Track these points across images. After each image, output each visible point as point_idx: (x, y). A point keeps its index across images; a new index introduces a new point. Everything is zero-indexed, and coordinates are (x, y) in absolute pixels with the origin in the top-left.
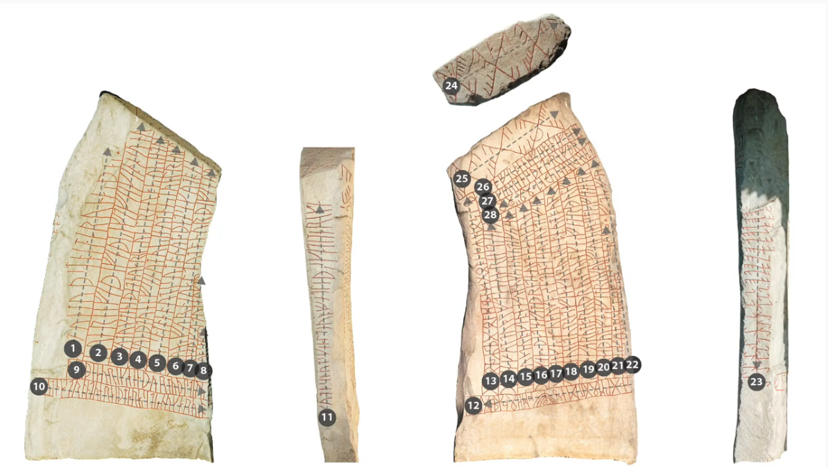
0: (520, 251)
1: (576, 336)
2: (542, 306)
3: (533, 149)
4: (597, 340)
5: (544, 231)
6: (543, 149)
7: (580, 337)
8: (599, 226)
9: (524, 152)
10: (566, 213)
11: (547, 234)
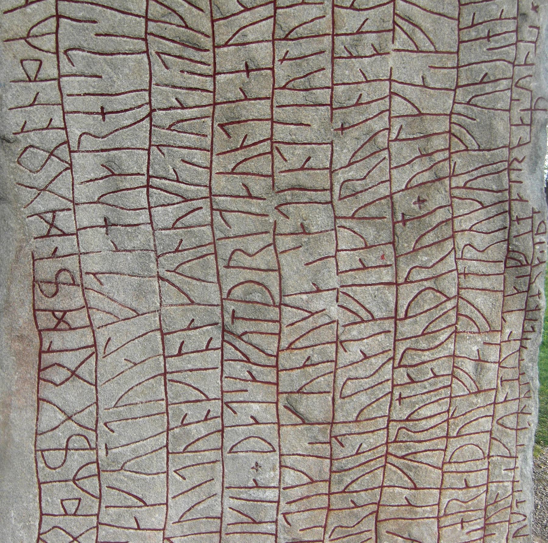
0: (208, 84)
1: (382, 422)
2: (273, 313)
4: (447, 437)
5: (315, 11)
7: (394, 428)
11: (325, 25)
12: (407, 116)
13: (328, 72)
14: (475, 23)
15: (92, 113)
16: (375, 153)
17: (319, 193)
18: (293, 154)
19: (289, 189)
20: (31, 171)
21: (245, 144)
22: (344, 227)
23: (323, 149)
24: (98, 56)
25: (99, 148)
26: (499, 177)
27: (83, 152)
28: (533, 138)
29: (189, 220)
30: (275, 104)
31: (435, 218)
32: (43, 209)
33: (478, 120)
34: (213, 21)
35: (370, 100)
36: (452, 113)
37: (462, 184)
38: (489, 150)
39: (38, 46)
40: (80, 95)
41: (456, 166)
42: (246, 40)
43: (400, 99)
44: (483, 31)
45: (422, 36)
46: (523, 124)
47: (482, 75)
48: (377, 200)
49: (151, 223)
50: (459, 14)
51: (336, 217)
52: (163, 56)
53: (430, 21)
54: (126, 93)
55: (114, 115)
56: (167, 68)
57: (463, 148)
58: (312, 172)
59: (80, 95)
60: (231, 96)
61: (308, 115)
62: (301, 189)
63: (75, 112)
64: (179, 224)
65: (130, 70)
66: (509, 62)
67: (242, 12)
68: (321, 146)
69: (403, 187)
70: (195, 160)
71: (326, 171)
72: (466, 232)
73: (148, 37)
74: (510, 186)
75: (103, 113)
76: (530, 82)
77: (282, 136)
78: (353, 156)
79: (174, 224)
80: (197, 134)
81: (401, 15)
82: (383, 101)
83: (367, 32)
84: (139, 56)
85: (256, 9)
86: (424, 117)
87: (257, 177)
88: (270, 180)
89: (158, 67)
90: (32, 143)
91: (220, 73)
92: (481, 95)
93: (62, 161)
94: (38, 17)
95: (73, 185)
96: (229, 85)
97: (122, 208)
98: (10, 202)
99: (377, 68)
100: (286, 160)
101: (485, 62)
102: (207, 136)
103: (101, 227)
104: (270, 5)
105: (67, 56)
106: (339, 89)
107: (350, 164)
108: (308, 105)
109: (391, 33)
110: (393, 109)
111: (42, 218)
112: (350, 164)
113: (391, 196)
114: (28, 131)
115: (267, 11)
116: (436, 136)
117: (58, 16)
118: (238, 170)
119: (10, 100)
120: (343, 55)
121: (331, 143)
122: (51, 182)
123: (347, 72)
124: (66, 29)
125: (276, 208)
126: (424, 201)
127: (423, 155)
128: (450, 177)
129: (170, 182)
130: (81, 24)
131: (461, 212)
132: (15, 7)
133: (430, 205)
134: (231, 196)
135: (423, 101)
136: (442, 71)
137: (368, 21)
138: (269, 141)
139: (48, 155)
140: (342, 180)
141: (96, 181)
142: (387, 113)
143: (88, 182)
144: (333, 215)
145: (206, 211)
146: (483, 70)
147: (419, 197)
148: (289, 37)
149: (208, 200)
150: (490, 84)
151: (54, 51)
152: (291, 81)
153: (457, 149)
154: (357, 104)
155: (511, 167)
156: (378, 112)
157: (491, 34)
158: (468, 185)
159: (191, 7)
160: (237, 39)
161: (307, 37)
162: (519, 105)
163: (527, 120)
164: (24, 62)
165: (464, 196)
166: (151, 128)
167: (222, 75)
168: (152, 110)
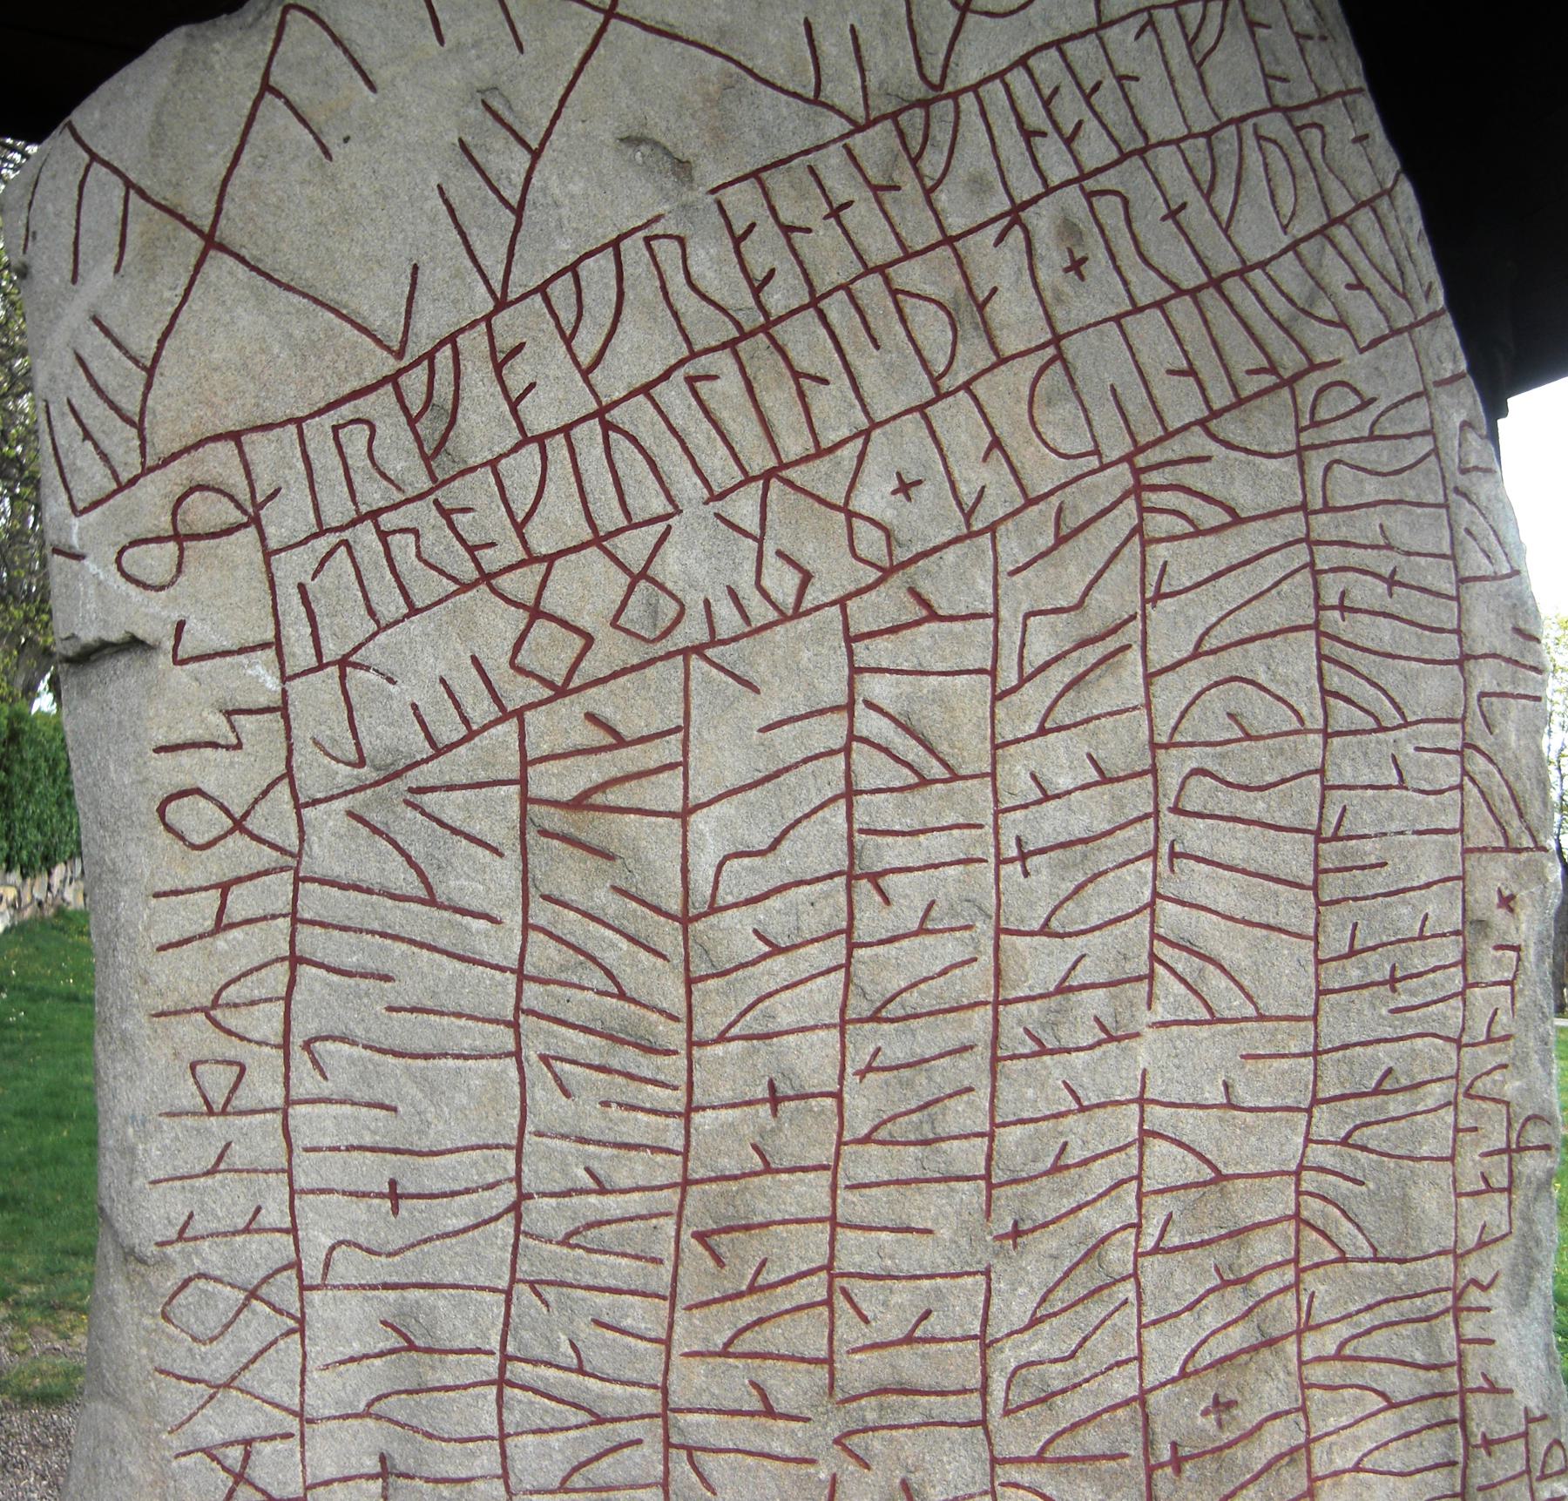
3: (937, 92)
5: (949, 949)
6: (1036, 118)
8: (1450, 951)
9: (845, 91)
10: (1171, 781)
11: (976, 981)
12: (1185, 1187)
13: (982, 1097)
14: (1357, 946)
15: (365, 1195)
16: (1100, 1289)
17: (952, 1398)
18: (885, 1304)
19: (872, 1393)
20: (194, 1339)
21: (760, 1281)
22: (1017, 1486)
23: (963, 1288)
24: (390, 1059)
25: (380, 1280)
26: (1430, 1331)
27: (335, 1287)
28: (1517, 1223)
29: (605, 1470)
30: (842, 1182)
31: (1261, 1448)
32: (219, 1437)
33: (1371, 1186)
34: (690, 982)
35: (1088, 1154)
36: (1301, 1167)
37: (1331, 1349)
38: (1401, 1261)
39: (240, 1031)
40: (338, 1149)
41: (1316, 1302)
42: (772, 1027)
43: (1165, 1144)
44: (1378, 967)
45: (1225, 982)
46: (1490, 1189)
47: (1378, 1075)
48: (1105, 1411)
49: (505, 1476)
50: (1317, 925)
51: (994, 1461)
52: (557, 1065)
53: (1243, 944)
54: (458, 1150)
55: (422, 1203)
56: (567, 1094)
57: (1333, 1254)
58: (934, 1347)
59: (338, 1149)
60: (729, 1165)
61: (925, 1206)
62: (904, 1391)
63: (322, 1191)
64: (578, 1481)
65: (471, 1097)
66: (1447, 1039)
67: (764, 957)
68: (960, 1281)
69: (1175, 1372)
70: (627, 1323)
71: (973, 1346)
72: (1346, 1477)
73: (522, 1017)
74: (1461, 1354)
75: (395, 1195)
76: (1504, 1082)
77: (857, 1259)
78: (1044, 1299)
79: (565, 1480)
80: (637, 1257)
81: (1171, 937)
82: (1122, 1155)
83: (1084, 987)
84: (495, 1063)
85: (802, 951)
86: (1229, 1186)
87: (789, 1365)
88: (822, 1373)
89: (543, 1094)
90: (203, 1268)
91: (704, 1109)
92: (1377, 1123)
93: (280, 1311)
94: (244, 961)
95: (303, 1371)
96: (723, 1136)
97: (430, 1436)
98: (133, 1412)
99: (1111, 1074)
100: (866, 1321)
101: (1386, 1040)
102: (661, 1262)
103: (370, 1477)
104: (836, 939)
105: (310, 1052)
106: (1010, 1137)
107: (1035, 1321)
108: (928, 1181)
109: (1145, 985)
110: (1147, 1172)
111: (214, 1458)
112: (1035, 1321)
113: (1142, 1398)
114: (195, 1238)
115: (829, 955)
116: (1260, 1232)
117: (295, 960)
118: (737, 1347)
119: (154, 1156)
120: (1022, 1050)
121: (987, 1273)
122: (246, 1367)
123: (1030, 1093)
124: (311, 991)
125: (837, 1441)
126: (1231, 1404)
127: (1226, 1283)
128: (1299, 1333)
129: (560, 1373)
130: (352, 981)
131: (1332, 1423)
132: (186, 935)
133: (1247, 1416)
134: (719, 1412)
135: (1225, 1145)
136: (1276, 1063)
137: (1086, 961)
138: (824, 1275)
139: (242, 1296)
140: (1013, 1365)
141: (366, 1362)
142: (1134, 1184)
143: (342, 1362)
144: (986, 1455)
145: (651, 1451)
146: (1379, 1061)
147: (1216, 1397)
148: (884, 1014)
149: (659, 1421)
150: (1400, 1097)
151: (280, 1040)
152: (884, 1122)
153: (1316, 1259)
154: (1057, 1168)
155: (1463, 1304)
156: (1110, 1183)
157: (1399, 974)
158: (1347, 1351)
159: (635, 948)
160: (750, 1024)
161: (930, 1014)
162: (1477, 1144)
163: (1499, 1180)
164: (199, 1068)
165: (1338, 1381)
166: (517, 1239)
167: (709, 1112)
168: (523, 1196)
